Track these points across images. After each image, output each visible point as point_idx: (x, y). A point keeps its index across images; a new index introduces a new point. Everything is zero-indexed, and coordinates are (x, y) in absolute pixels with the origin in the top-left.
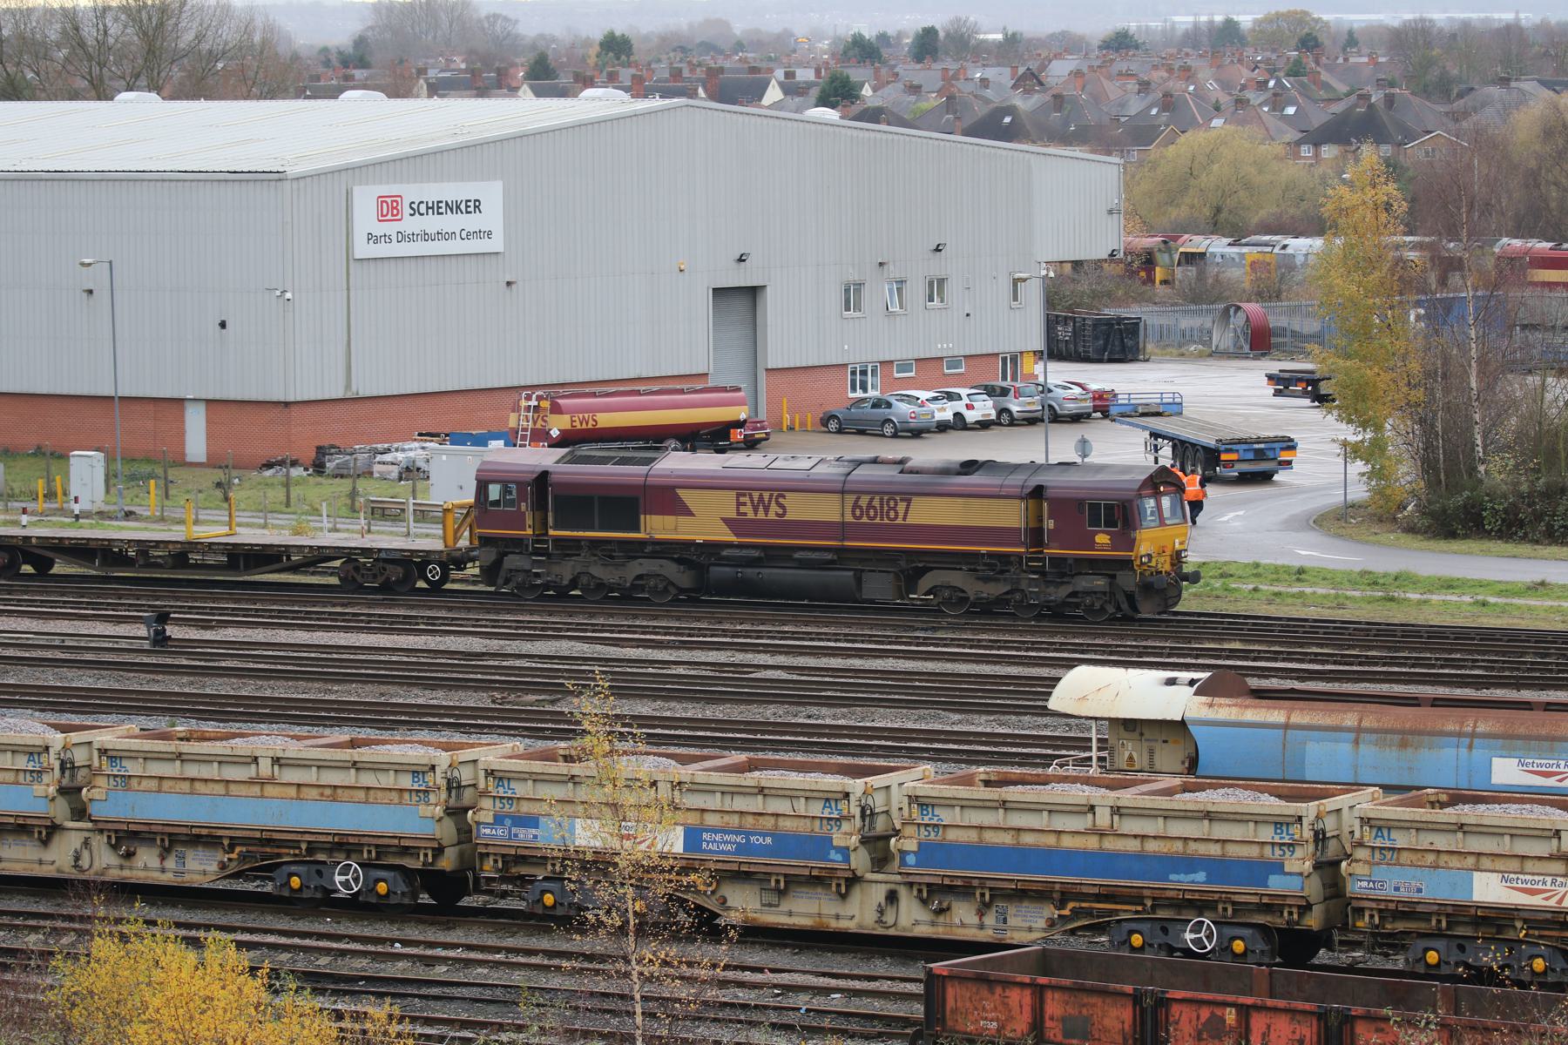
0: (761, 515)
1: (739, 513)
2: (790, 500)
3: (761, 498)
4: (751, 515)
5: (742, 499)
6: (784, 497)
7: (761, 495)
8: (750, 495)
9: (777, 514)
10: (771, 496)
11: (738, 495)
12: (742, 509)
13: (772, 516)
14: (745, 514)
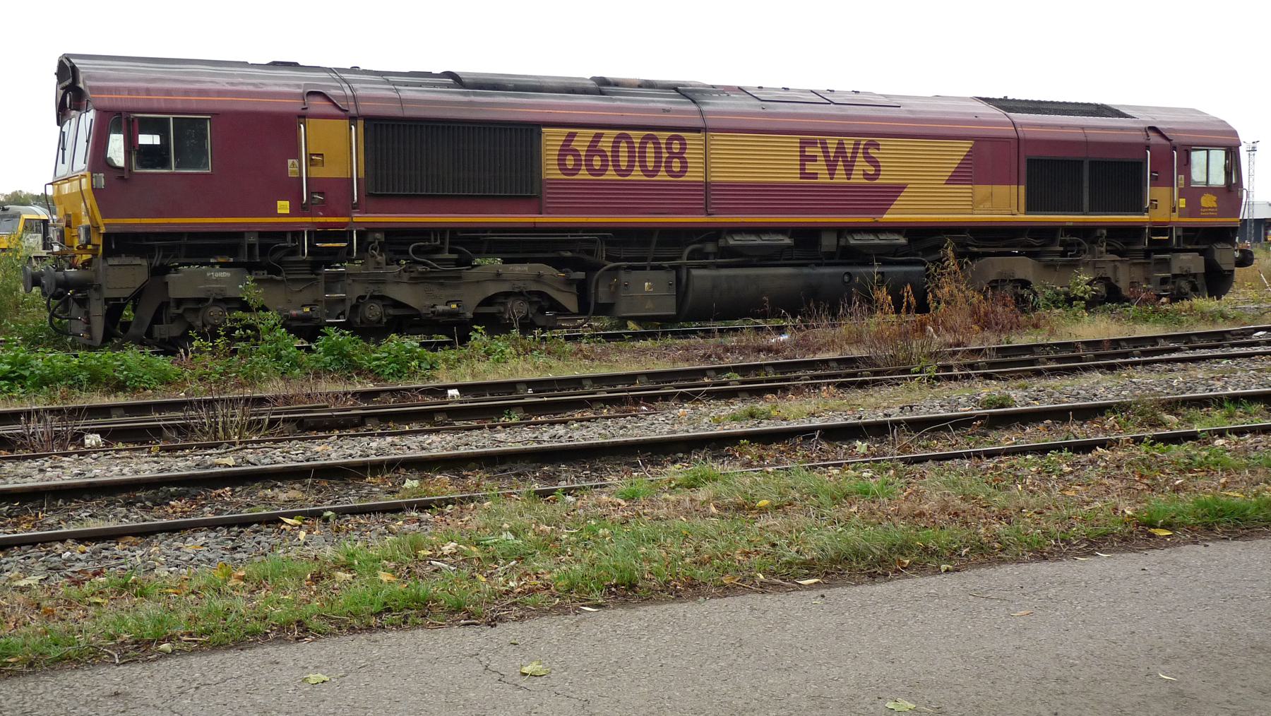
0: (840, 177)
1: (804, 175)
2: (887, 151)
3: (841, 147)
4: (824, 178)
5: (810, 151)
6: (877, 146)
7: (841, 146)
8: (823, 143)
9: (866, 175)
10: (857, 144)
11: (804, 144)
12: (810, 167)
13: (857, 178)
14: (814, 176)
